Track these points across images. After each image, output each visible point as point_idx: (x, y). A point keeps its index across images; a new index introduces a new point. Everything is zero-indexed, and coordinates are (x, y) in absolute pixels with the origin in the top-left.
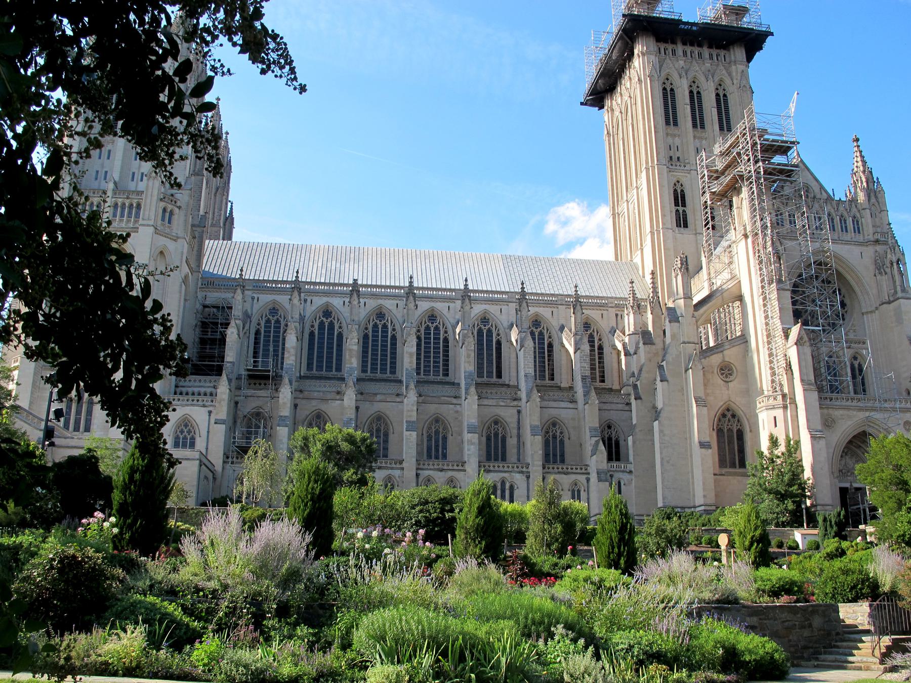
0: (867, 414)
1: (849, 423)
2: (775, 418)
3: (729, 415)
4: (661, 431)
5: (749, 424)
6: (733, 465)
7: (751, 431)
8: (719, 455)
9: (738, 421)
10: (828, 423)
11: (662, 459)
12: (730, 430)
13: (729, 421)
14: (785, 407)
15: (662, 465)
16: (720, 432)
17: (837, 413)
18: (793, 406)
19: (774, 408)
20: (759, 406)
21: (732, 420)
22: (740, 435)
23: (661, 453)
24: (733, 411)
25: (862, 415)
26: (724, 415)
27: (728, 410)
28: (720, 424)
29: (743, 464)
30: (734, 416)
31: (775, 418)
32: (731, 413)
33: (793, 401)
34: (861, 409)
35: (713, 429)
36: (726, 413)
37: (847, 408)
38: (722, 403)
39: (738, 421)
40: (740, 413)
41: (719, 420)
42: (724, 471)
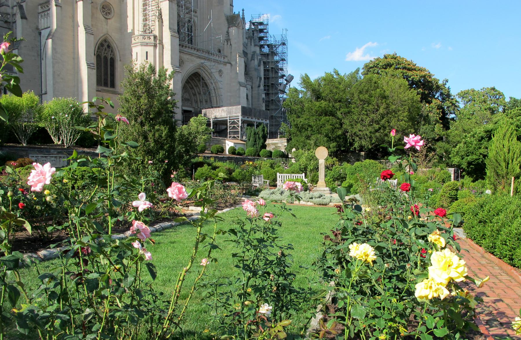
0: (202, 61)
1: (191, 65)
2: (147, 52)
3: (106, 46)
4: (54, 49)
5: (120, 55)
6: (106, 85)
7: (120, 60)
8: (97, 75)
9: (112, 51)
10: (181, 63)
11: (54, 72)
12: (106, 58)
13: (105, 50)
14: (155, 46)
15: (54, 77)
16: (98, 57)
17: (185, 57)
18: (161, 46)
19: (147, 45)
20: (133, 42)
21: (107, 49)
22: (113, 61)
23: (53, 67)
24: (109, 43)
25: (199, 61)
26: (102, 45)
27: (105, 41)
28: (99, 51)
29: (113, 85)
30: (109, 46)
31: (147, 52)
32: (107, 44)
33: (161, 43)
34: (199, 57)
35: (95, 54)
36: (104, 43)
37: (191, 54)
38: (102, 35)
39: (112, 51)
40: (114, 45)
41: (99, 48)
42: (100, 88)
